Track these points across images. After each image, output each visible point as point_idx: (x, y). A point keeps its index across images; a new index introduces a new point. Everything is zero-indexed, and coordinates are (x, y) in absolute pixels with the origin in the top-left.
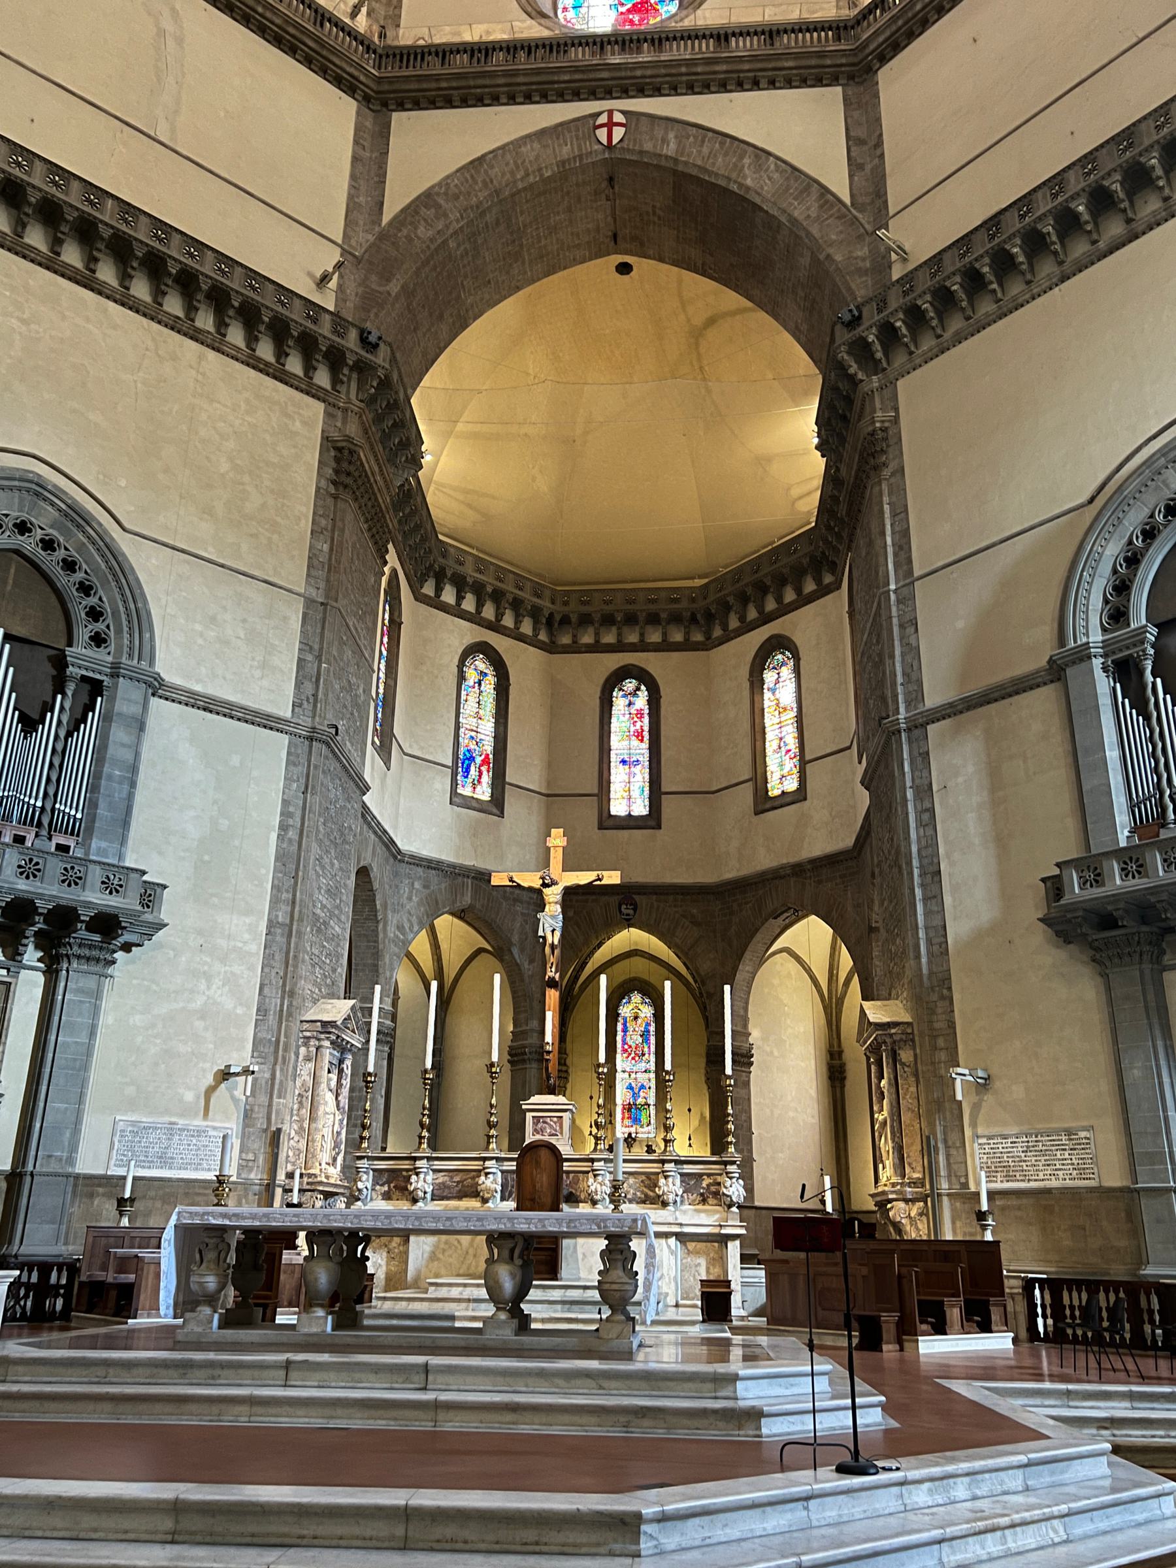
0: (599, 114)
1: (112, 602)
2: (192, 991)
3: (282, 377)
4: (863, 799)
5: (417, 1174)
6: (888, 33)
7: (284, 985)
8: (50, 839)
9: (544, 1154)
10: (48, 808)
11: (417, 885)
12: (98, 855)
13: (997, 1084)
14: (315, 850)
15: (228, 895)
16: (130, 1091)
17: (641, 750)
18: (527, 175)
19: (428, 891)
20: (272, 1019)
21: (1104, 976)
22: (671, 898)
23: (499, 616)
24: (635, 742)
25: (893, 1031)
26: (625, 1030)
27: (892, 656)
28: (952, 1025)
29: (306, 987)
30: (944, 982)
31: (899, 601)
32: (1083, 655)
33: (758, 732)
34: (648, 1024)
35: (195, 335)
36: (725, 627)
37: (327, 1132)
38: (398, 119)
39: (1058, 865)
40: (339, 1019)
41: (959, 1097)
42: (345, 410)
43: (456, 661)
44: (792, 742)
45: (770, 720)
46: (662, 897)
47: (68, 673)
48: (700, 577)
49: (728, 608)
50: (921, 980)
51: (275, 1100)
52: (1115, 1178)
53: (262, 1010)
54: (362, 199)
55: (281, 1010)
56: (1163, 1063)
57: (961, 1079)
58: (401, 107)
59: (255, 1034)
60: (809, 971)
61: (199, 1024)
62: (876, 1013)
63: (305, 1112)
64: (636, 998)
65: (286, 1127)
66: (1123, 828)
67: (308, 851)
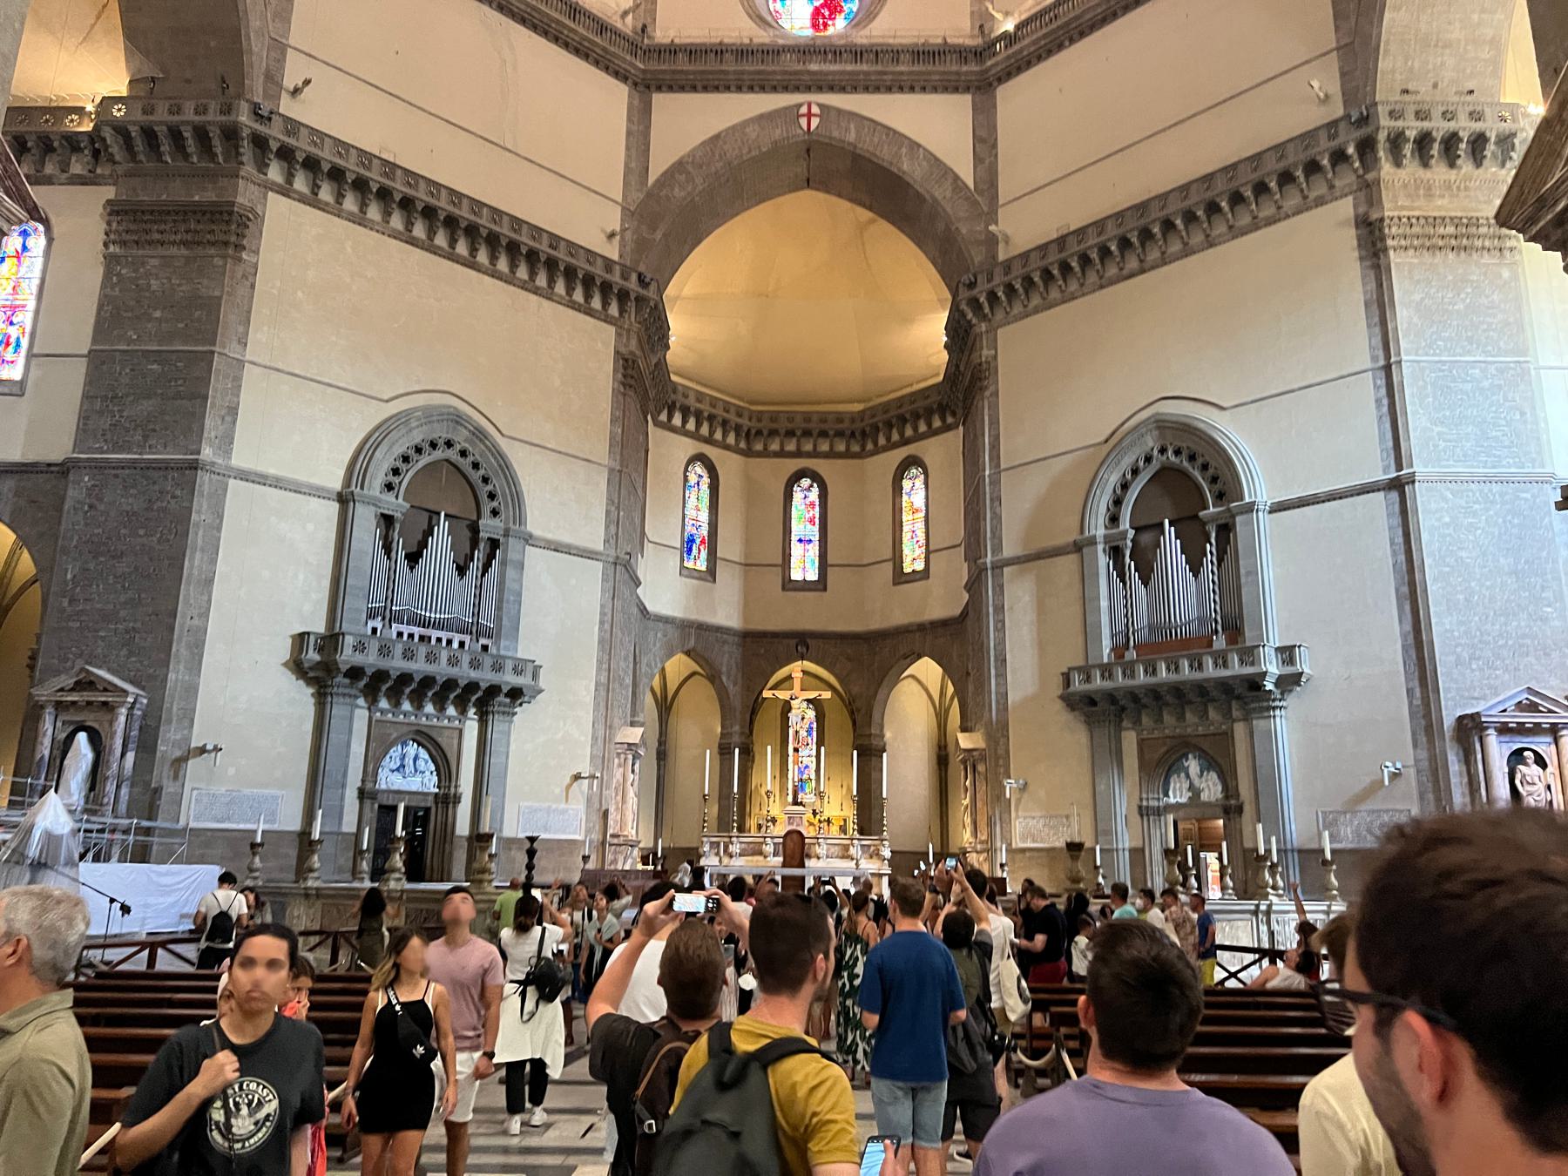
0: (800, 105)
1: (502, 487)
3: (589, 312)
4: (966, 596)
6: (1004, 66)
9: (795, 836)
11: (659, 635)
13: (1031, 788)
17: (814, 532)
18: (750, 151)
20: (600, 742)
23: (712, 433)
24: (809, 526)
27: (985, 519)
30: (1004, 726)
31: (990, 483)
32: (1092, 542)
33: (897, 526)
35: (536, 291)
36: (876, 443)
38: (658, 99)
42: (628, 331)
44: (921, 536)
45: (906, 517)
48: (859, 401)
49: (877, 430)
53: (594, 738)
54: (633, 165)
57: (1010, 785)
58: (659, 89)
62: (965, 741)
63: (619, 798)
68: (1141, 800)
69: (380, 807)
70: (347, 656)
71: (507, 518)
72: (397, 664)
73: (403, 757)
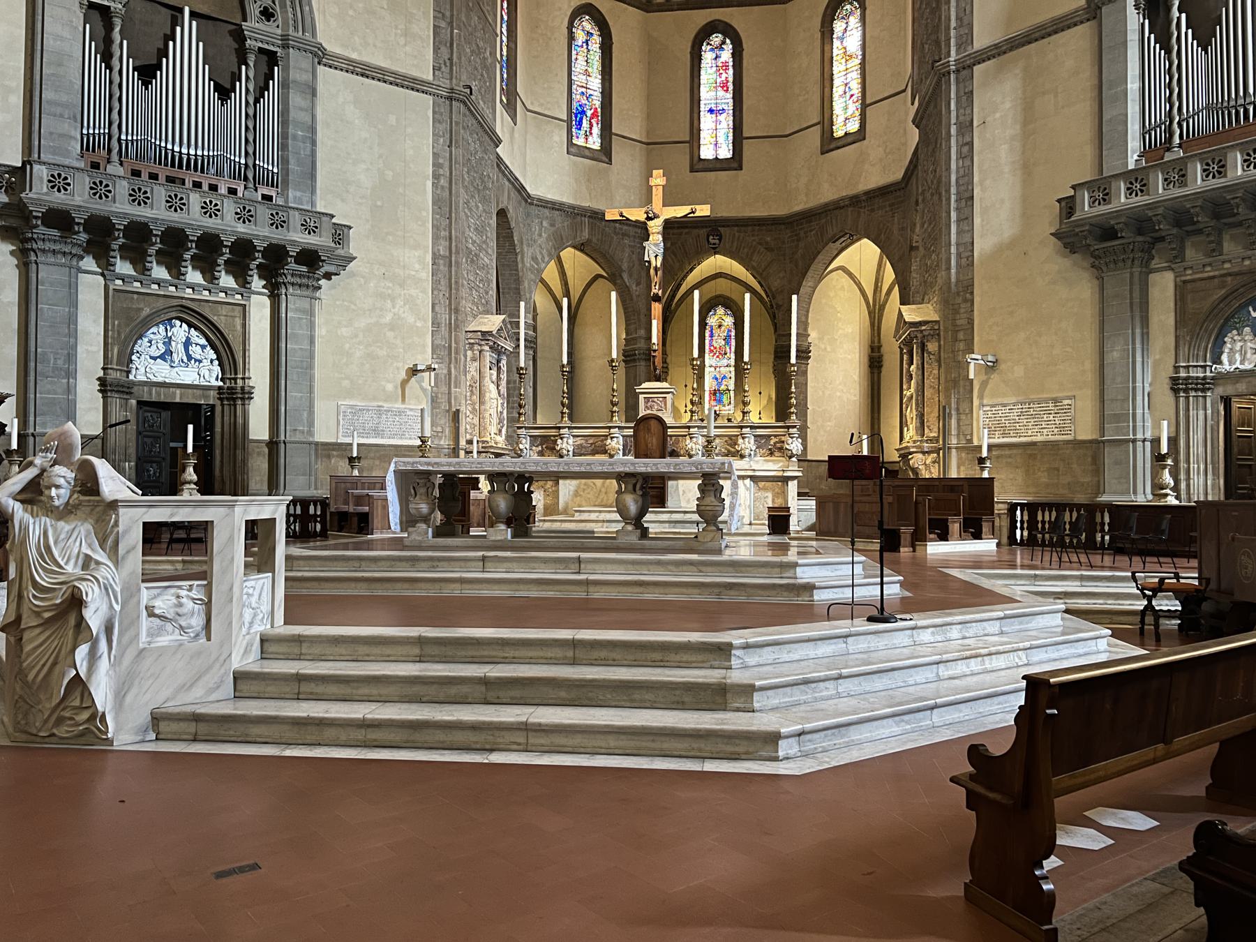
2: (381, 310)
4: (914, 135)
5: (562, 439)
7: (450, 304)
8: (256, 190)
9: (653, 423)
10: (251, 165)
11: (545, 224)
12: (295, 202)
13: (1003, 366)
14: (463, 196)
15: (400, 233)
16: (346, 383)
17: (727, 99)
19: (553, 229)
20: (444, 330)
21: (1100, 278)
22: (750, 228)
24: (721, 93)
25: (923, 328)
26: (711, 336)
28: (971, 322)
29: (466, 305)
30: (967, 288)
33: (827, 79)
34: (729, 331)
37: (493, 411)
39: (1074, 187)
40: (494, 329)
41: (971, 376)
43: (566, 23)
44: (855, 87)
45: (838, 68)
46: (743, 228)
47: (247, 46)
50: (950, 288)
51: (453, 390)
52: (1086, 432)
53: (436, 323)
55: (450, 324)
56: (1138, 346)
57: (974, 364)
59: (433, 342)
60: (859, 285)
61: (390, 334)
62: (911, 314)
63: (476, 398)
64: (720, 311)
65: (463, 409)
66: (1133, 152)
67: (458, 196)
68: (1176, 369)
69: (140, 403)
70: (39, 192)
71: (286, 22)
72: (121, 207)
73: (168, 341)
